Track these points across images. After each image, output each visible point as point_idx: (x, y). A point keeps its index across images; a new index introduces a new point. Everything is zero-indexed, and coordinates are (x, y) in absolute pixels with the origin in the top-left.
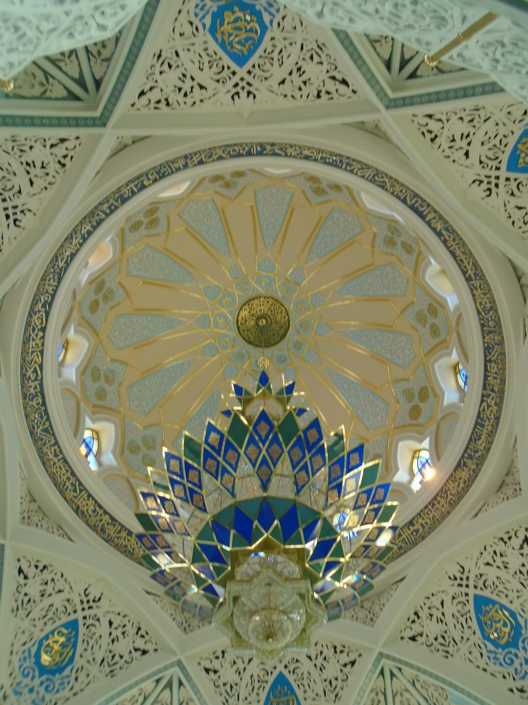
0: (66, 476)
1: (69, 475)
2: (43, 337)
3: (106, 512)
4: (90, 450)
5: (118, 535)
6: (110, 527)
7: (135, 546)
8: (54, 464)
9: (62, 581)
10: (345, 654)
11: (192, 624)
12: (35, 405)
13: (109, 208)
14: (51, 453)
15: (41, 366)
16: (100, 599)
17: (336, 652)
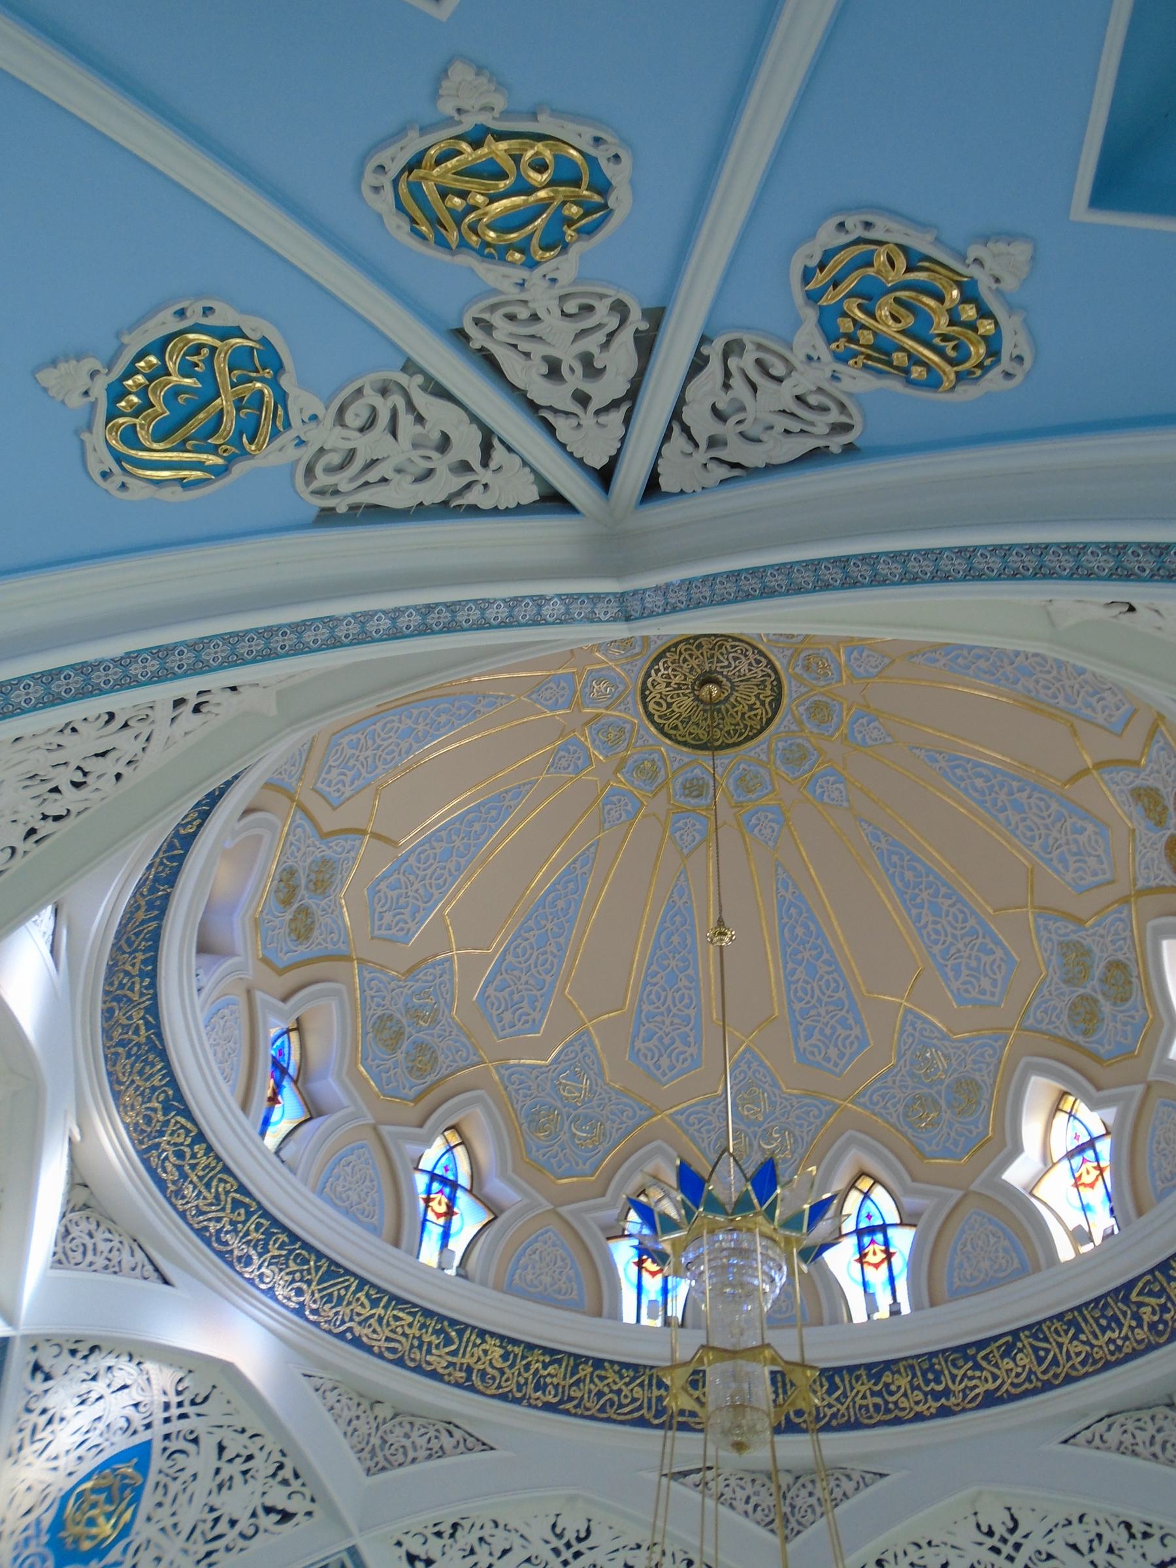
0: (416, 1325)
1: (422, 1320)
2: (210, 1149)
3: (531, 1347)
4: (454, 1185)
5: (575, 1378)
6: (551, 1369)
7: (620, 1385)
8: (380, 1319)
9: (500, 1532)
10: (1154, 1542)
11: (798, 1502)
12: (276, 1253)
13: (150, 906)
14: (362, 1305)
15: (242, 1189)
16: (588, 1532)
17: (1132, 1536)
